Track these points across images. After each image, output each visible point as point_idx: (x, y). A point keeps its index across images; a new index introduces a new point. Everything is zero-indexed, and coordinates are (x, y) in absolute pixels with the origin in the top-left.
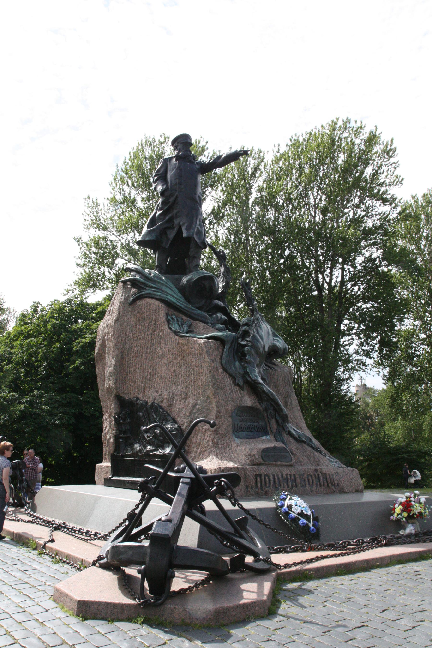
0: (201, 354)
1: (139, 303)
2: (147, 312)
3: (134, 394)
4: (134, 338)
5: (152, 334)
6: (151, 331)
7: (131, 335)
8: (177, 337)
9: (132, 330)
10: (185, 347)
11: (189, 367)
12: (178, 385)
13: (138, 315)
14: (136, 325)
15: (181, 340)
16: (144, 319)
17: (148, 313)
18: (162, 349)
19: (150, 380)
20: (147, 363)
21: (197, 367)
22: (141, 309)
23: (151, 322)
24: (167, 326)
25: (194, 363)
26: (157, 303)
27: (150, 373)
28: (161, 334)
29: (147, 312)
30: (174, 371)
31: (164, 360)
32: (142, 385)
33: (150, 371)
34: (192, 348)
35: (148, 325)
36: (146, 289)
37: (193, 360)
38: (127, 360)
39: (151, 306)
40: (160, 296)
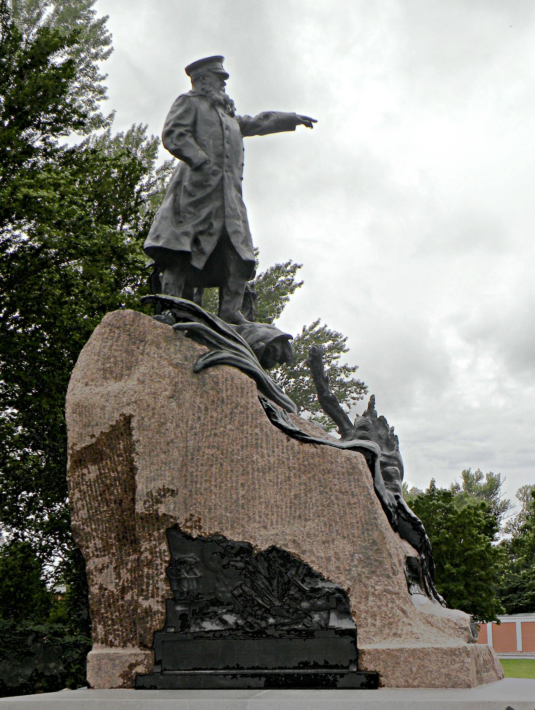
0: (349, 474)
1: (212, 371)
2: (227, 390)
3: (210, 528)
4: (203, 431)
5: (237, 428)
6: (236, 422)
7: (198, 426)
8: (293, 441)
9: (199, 418)
10: (317, 459)
11: (327, 493)
12: (306, 520)
13: (211, 392)
14: (206, 409)
15: (307, 447)
16: (223, 400)
17: (229, 393)
18: (263, 456)
19: (242, 508)
20: (234, 478)
21: (343, 493)
22: (217, 383)
23: (236, 408)
24: (268, 420)
25: (338, 487)
26: (245, 376)
27: (243, 496)
28: (257, 430)
29: (227, 390)
30: (296, 496)
31: (270, 476)
32: (228, 515)
33: (242, 493)
34: (332, 463)
35: (231, 413)
36: (221, 349)
37: (336, 481)
38: (190, 469)
39: (235, 382)
40: (248, 364)
